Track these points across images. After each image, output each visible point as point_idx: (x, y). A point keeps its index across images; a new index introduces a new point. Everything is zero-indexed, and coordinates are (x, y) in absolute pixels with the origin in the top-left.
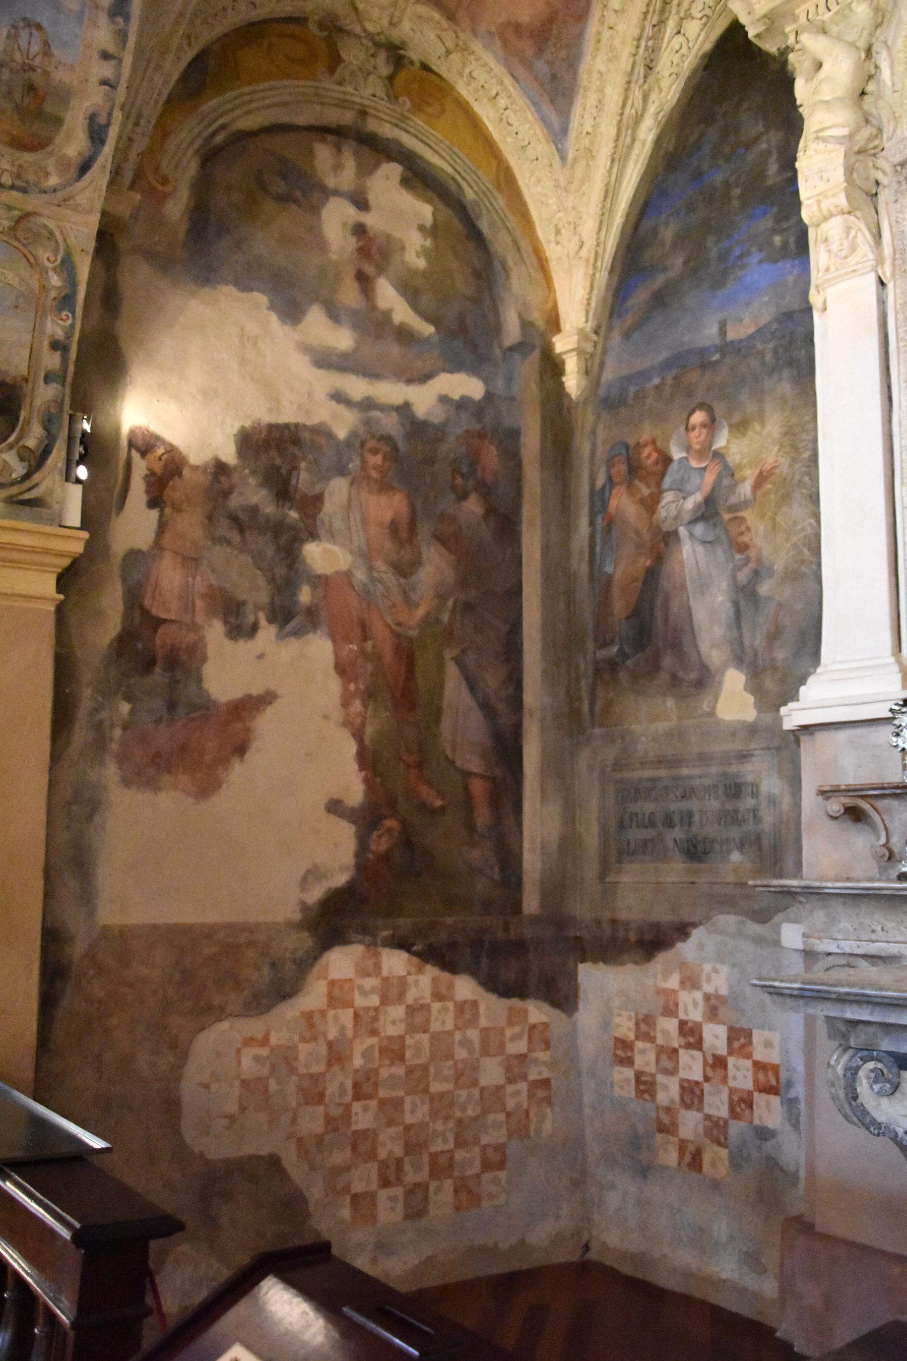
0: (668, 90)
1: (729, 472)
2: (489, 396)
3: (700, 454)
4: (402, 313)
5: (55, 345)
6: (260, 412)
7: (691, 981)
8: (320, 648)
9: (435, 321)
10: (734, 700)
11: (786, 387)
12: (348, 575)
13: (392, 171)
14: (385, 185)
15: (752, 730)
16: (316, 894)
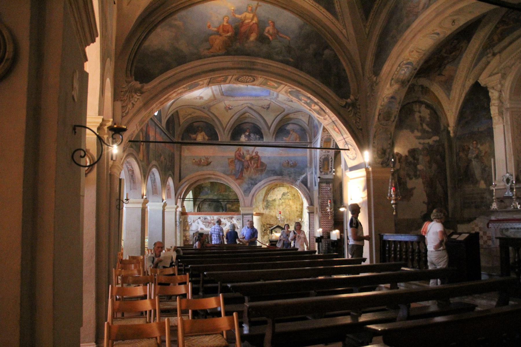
0: (467, 89)
1: (481, 151)
2: (440, 139)
3: (475, 148)
4: (427, 129)
5: (390, 144)
6: (410, 147)
7: (477, 226)
8: (420, 180)
9: (432, 129)
10: (482, 185)
11: (489, 138)
12: (423, 170)
13: (423, 106)
14: (423, 108)
15: (485, 190)
16: (423, 214)
